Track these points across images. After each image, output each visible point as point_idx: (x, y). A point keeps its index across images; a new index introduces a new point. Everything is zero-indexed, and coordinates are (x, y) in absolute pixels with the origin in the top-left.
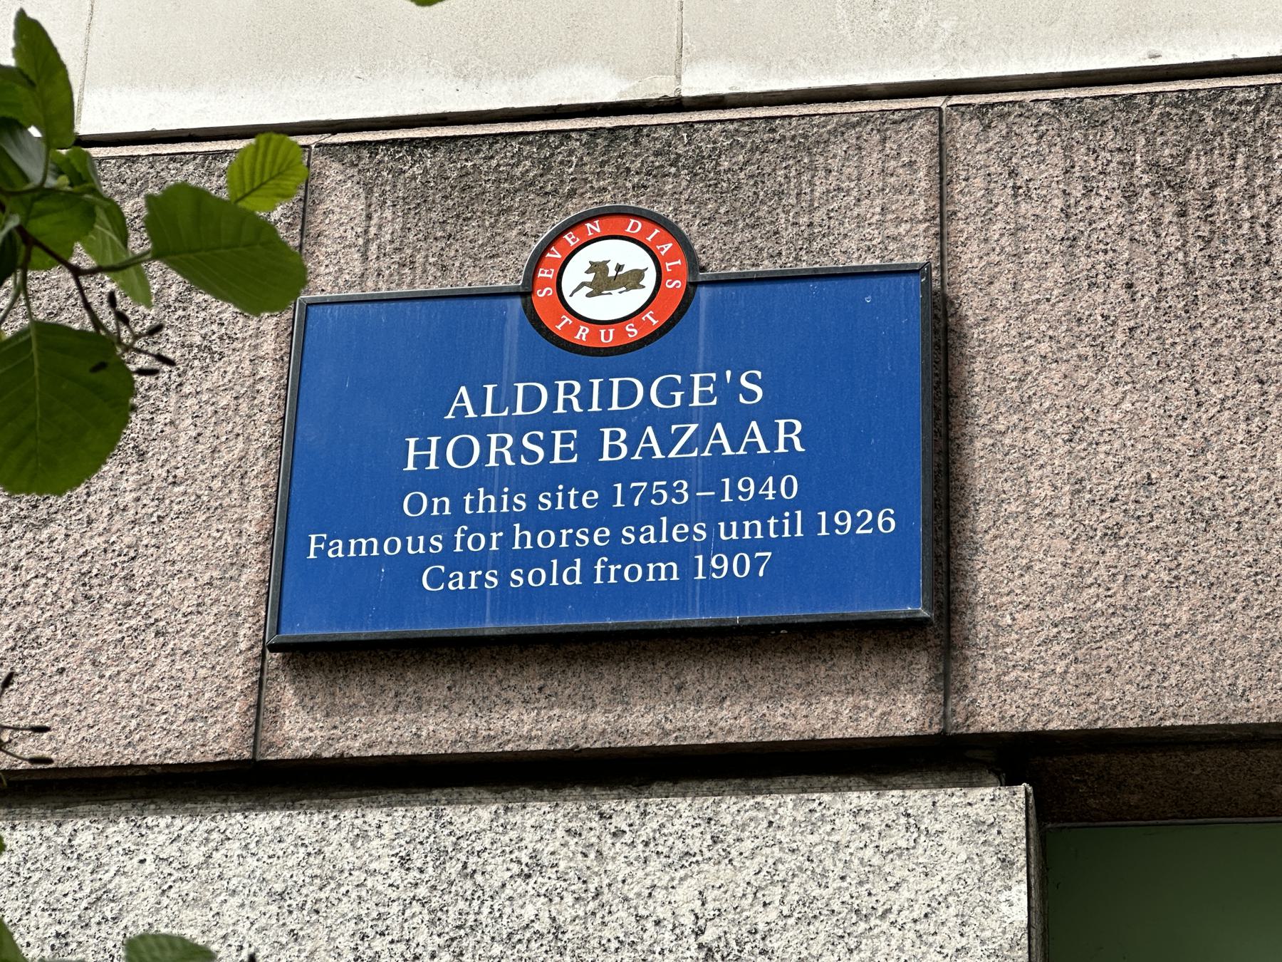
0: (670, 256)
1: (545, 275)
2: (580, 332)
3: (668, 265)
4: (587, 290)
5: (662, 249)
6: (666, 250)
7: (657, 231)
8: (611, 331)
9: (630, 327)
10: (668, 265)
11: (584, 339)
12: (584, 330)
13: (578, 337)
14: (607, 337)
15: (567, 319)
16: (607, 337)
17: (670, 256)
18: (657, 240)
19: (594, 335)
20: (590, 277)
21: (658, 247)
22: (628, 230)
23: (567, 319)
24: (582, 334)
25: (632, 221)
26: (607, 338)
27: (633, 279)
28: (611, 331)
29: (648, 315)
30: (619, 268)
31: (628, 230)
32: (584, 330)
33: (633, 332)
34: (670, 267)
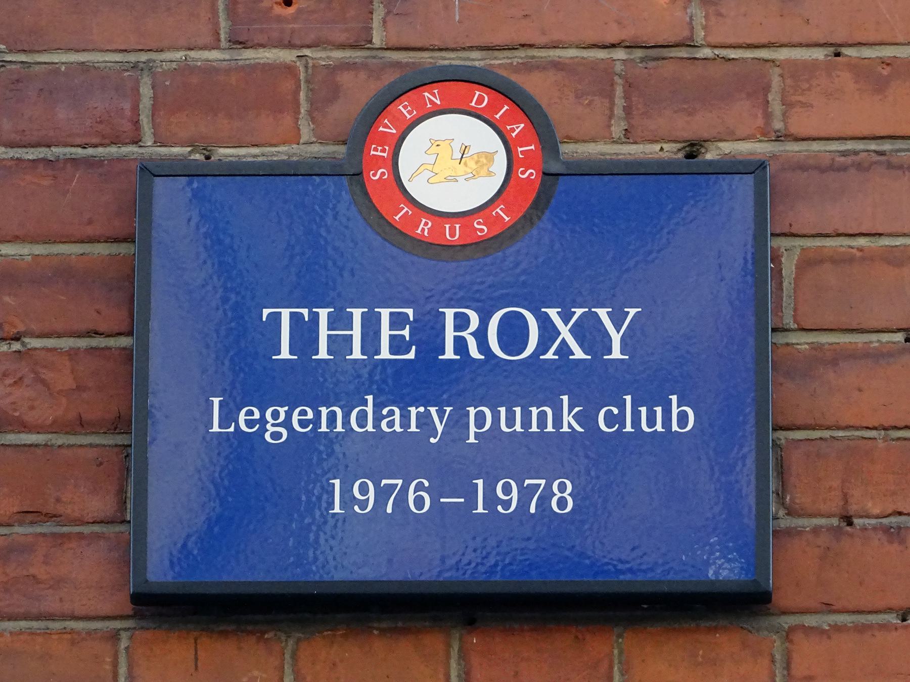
0: (522, 139)
3: (520, 149)
5: (513, 130)
6: (517, 131)
9: (479, 223)
11: (426, 233)
12: (426, 224)
13: (419, 231)
14: (452, 234)
15: (406, 209)
16: (452, 234)
17: (522, 139)
19: (437, 230)
22: (473, 104)
24: (424, 228)
26: (453, 234)
29: (498, 210)
32: (426, 224)
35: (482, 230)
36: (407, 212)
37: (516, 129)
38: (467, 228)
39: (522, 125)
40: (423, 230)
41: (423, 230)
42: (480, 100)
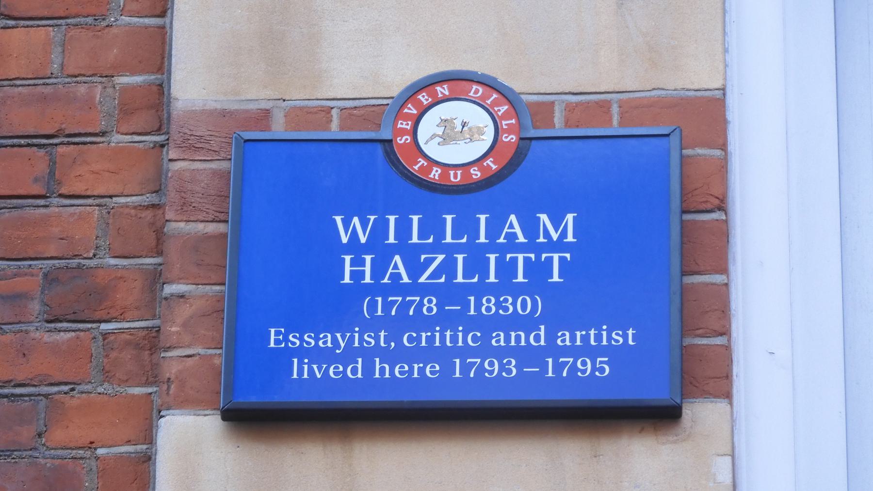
0: (505, 116)
1: (404, 126)
2: (434, 172)
3: (504, 123)
4: (438, 140)
5: (499, 110)
6: (502, 111)
7: (495, 96)
8: (459, 172)
10: (504, 123)
11: (437, 178)
12: (437, 171)
13: (431, 176)
14: (455, 177)
16: (455, 177)
17: (505, 116)
18: (495, 103)
19: (444, 175)
20: (440, 131)
21: (496, 109)
23: (422, 162)
24: (435, 174)
25: (475, 87)
26: (454, 178)
27: (474, 134)
28: (459, 172)
29: (488, 162)
30: (464, 125)
31: (471, 94)
32: (437, 171)
33: (476, 173)
34: (506, 125)
35: (476, 175)
36: (423, 164)
37: (501, 110)
38: (467, 175)
39: (506, 107)
40: (434, 175)
41: (434, 175)
42: (477, 92)
